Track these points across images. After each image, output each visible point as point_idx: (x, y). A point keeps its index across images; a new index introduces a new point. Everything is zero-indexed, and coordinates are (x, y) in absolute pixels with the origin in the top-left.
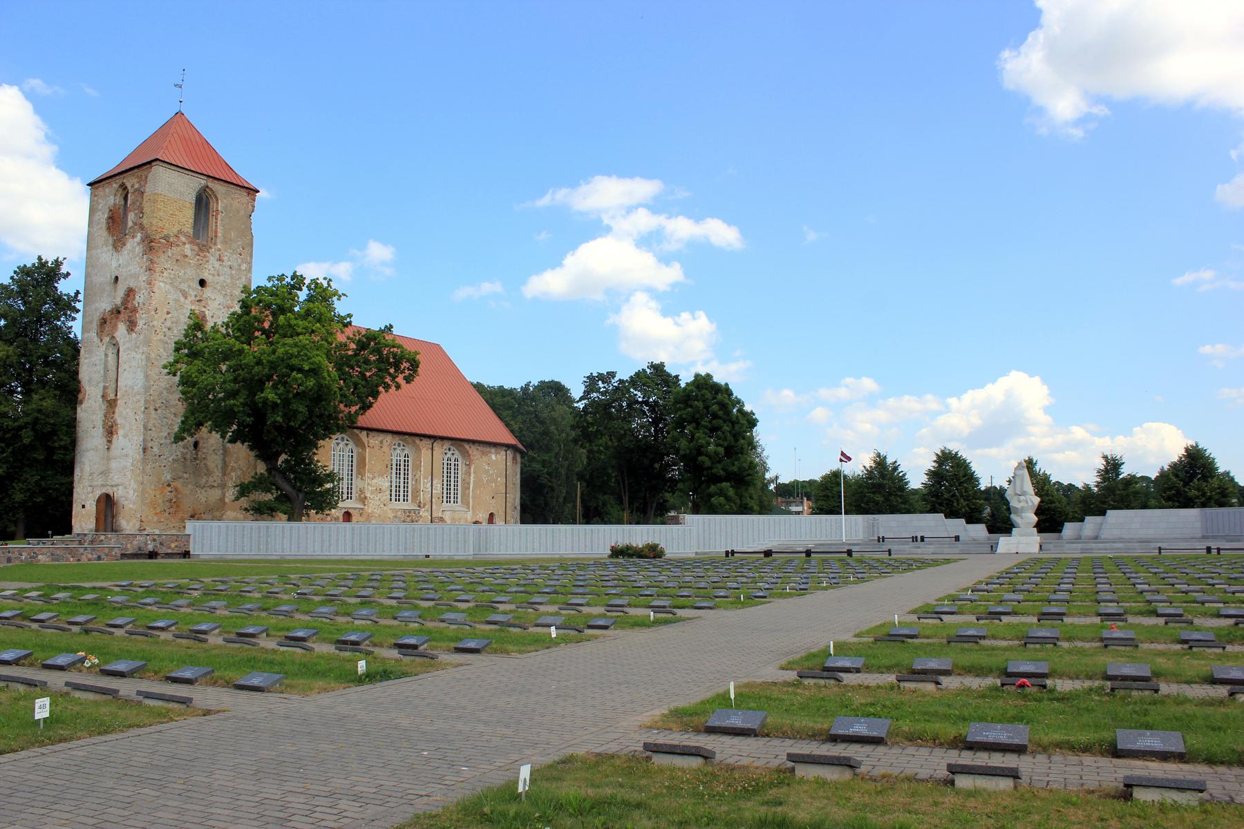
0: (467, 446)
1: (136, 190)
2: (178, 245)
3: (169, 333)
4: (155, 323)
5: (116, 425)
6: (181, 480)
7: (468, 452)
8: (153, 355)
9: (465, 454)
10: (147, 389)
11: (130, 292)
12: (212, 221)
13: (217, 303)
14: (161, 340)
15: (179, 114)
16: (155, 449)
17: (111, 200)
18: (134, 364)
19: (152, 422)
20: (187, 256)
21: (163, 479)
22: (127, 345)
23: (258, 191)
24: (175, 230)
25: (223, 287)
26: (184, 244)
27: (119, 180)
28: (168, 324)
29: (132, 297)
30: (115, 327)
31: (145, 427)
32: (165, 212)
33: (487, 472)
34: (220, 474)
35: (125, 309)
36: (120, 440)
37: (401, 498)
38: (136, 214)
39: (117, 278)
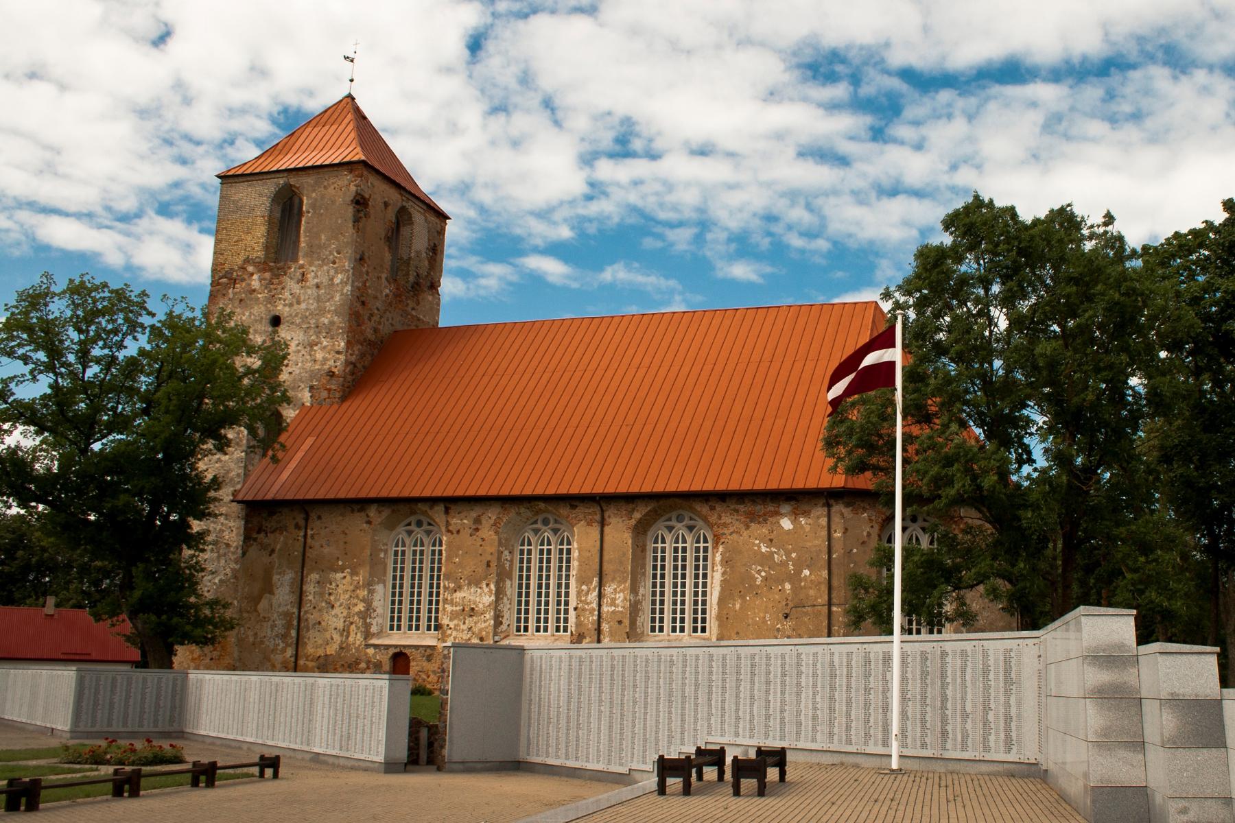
15: (350, 97)
20: (254, 291)
24: (240, 261)
25: (304, 318)
26: (252, 274)
32: (227, 241)
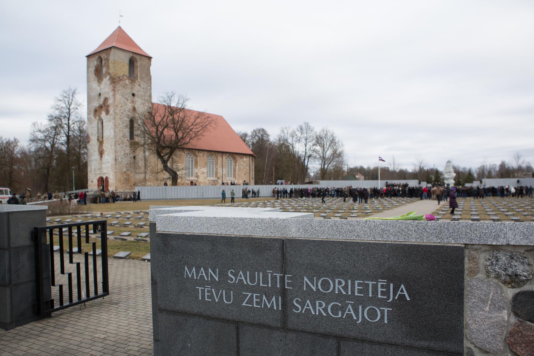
0: (235, 155)
1: (105, 59)
2: (123, 80)
3: (122, 115)
4: (117, 111)
5: (104, 150)
6: (130, 171)
7: (235, 157)
8: (117, 124)
9: (235, 159)
10: (115, 136)
11: (106, 99)
12: (135, 70)
13: (139, 103)
14: (119, 118)
15: (120, 27)
16: (120, 160)
17: (95, 63)
18: (109, 127)
19: (118, 149)
21: (123, 170)
22: (106, 120)
23: (152, 58)
24: (122, 74)
26: (126, 80)
27: (98, 55)
28: (122, 111)
29: (107, 101)
30: (101, 113)
31: (116, 151)
33: (242, 165)
34: (144, 169)
35: (105, 106)
36: (105, 156)
37: (211, 176)
38: (106, 68)
39: (100, 94)
